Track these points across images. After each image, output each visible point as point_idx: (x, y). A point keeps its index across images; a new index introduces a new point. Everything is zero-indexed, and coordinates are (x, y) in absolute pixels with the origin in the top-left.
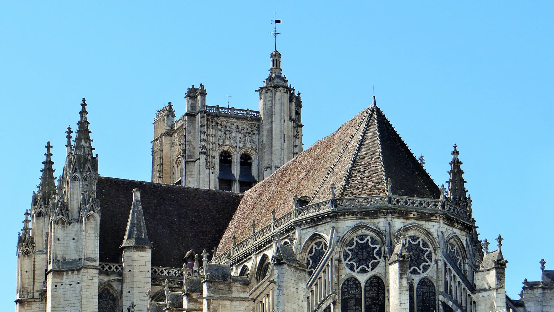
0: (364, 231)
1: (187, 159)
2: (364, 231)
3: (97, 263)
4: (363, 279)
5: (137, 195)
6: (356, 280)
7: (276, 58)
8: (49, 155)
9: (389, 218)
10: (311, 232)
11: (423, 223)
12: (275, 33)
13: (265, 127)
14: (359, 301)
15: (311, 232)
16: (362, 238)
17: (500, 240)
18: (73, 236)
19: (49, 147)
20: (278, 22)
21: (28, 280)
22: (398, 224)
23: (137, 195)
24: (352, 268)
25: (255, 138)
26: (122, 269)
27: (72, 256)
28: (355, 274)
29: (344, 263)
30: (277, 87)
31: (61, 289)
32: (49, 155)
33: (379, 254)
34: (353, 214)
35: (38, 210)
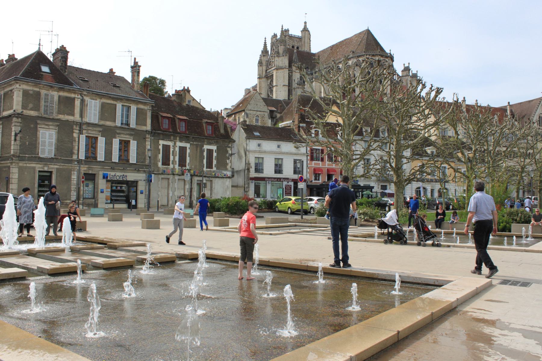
0: (372, 60)
2: (372, 60)
3: (288, 67)
7: (305, 23)
8: (265, 40)
13: (303, 40)
17: (409, 63)
19: (265, 38)
21: (261, 72)
25: (300, 43)
27: (281, 65)
30: (306, 30)
31: (278, 74)
32: (265, 40)
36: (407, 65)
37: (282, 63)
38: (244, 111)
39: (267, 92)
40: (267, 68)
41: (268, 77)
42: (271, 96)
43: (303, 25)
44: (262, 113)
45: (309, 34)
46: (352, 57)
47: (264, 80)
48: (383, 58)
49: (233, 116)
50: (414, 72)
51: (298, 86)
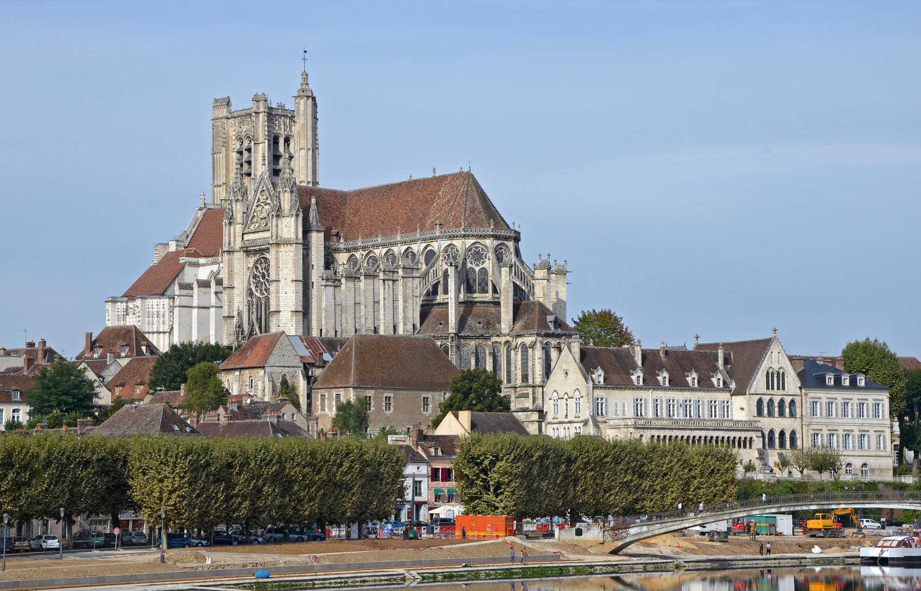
1: (255, 142)
2: (478, 245)
4: (477, 269)
5: (313, 201)
6: (474, 269)
7: (305, 76)
9: (492, 239)
10: (449, 242)
11: (505, 242)
12: (304, 59)
14: (475, 281)
15: (449, 242)
16: (477, 248)
18: (285, 224)
20: (305, 52)
22: (496, 243)
23: (313, 201)
24: (471, 263)
26: (308, 242)
28: (473, 266)
29: (468, 260)
30: (308, 97)
33: (486, 257)
34: (473, 236)
35: (237, 198)
36: (545, 258)
37: (288, 232)
38: (263, 367)
39: (246, 284)
40: (244, 229)
41: (250, 251)
42: (258, 294)
43: (300, 81)
44: (292, 369)
45: (315, 105)
46: (439, 237)
47: (239, 256)
48: (500, 242)
49: (237, 373)
50: (561, 262)
51: (324, 283)
